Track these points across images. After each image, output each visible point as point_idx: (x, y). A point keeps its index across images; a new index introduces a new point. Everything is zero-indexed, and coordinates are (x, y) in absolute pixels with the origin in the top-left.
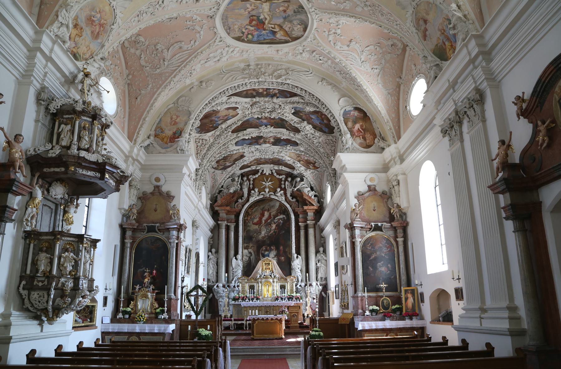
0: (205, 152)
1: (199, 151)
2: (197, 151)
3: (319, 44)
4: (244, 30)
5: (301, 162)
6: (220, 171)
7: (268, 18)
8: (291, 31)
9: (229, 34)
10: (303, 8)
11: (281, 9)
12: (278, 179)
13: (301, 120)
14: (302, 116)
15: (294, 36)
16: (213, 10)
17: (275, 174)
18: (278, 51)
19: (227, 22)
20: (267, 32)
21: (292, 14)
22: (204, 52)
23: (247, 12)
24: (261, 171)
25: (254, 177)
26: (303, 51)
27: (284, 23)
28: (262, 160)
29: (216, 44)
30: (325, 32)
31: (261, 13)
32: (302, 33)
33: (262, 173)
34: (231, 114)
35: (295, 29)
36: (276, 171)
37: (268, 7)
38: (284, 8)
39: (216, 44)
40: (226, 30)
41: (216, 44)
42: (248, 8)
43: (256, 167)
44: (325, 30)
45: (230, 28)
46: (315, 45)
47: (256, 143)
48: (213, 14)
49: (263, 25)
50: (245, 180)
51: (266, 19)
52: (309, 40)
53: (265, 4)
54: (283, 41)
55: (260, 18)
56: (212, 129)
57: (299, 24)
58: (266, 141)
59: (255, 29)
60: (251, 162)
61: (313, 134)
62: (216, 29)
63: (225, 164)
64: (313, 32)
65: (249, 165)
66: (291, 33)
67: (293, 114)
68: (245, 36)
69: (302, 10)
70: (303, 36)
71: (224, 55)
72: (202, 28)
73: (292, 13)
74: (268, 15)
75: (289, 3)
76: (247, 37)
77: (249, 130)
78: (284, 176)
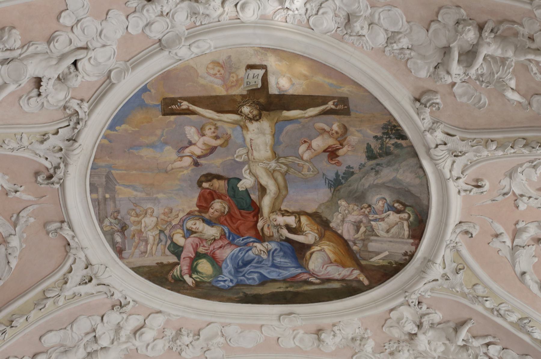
3: (480, 290)
4: (179, 239)
7: (272, 188)
8: (365, 240)
9: (120, 252)
10: (402, 136)
11: (319, 143)
15: (376, 260)
16: (53, 141)
18: (319, 332)
19: (113, 199)
20: (272, 246)
21: (362, 166)
22: (20, 322)
23: (187, 161)
26: (420, 326)
27: (332, 203)
29: (68, 293)
30: (497, 236)
31: (244, 163)
32: (408, 248)
35: (380, 227)
37: (269, 139)
38: (331, 142)
39: (68, 293)
40: (109, 235)
41: (71, 288)
42: (191, 143)
44: (500, 229)
45: (124, 228)
46: (464, 295)
48: (55, 159)
49: (251, 219)
51: (263, 190)
52: (436, 271)
53: (253, 126)
54: (336, 285)
55: (242, 186)
57: (391, 208)
59: (223, 236)
62: (71, 227)
64: (449, 236)
66: (365, 246)
68: (185, 266)
69: (396, 146)
70: (412, 256)
71: (104, 342)
72: (15, 225)
73: (362, 158)
74: (271, 173)
75: (345, 119)
76: (193, 270)
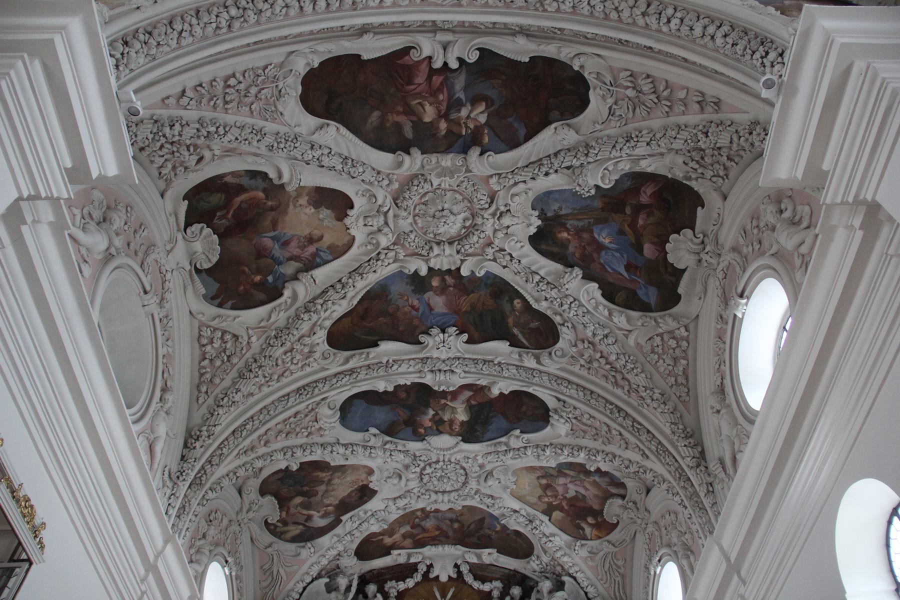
0: (227, 382)
1: (208, 376)
2: (202, 375)
5: (557, 515)
6: (292, 547)
12: (480, 592)
13: (559, 267)
14: (564, 245)
17: (469, 579)
24: (422, 568)
25: (402, 586)
28: (429, 524)
33: (426, 575)
34: (327, 240)
36: (474, 569)
43: (409, 556)
47: (409, 430)
50: (370, 594)
56: (261, 296)
58: (441, 421)
60: (390, 532)
61: (603, 327)
63: (309, 518)
65: (388, 541)
67: (537, 241)
77: (388, 348)
78: (498, 584)
